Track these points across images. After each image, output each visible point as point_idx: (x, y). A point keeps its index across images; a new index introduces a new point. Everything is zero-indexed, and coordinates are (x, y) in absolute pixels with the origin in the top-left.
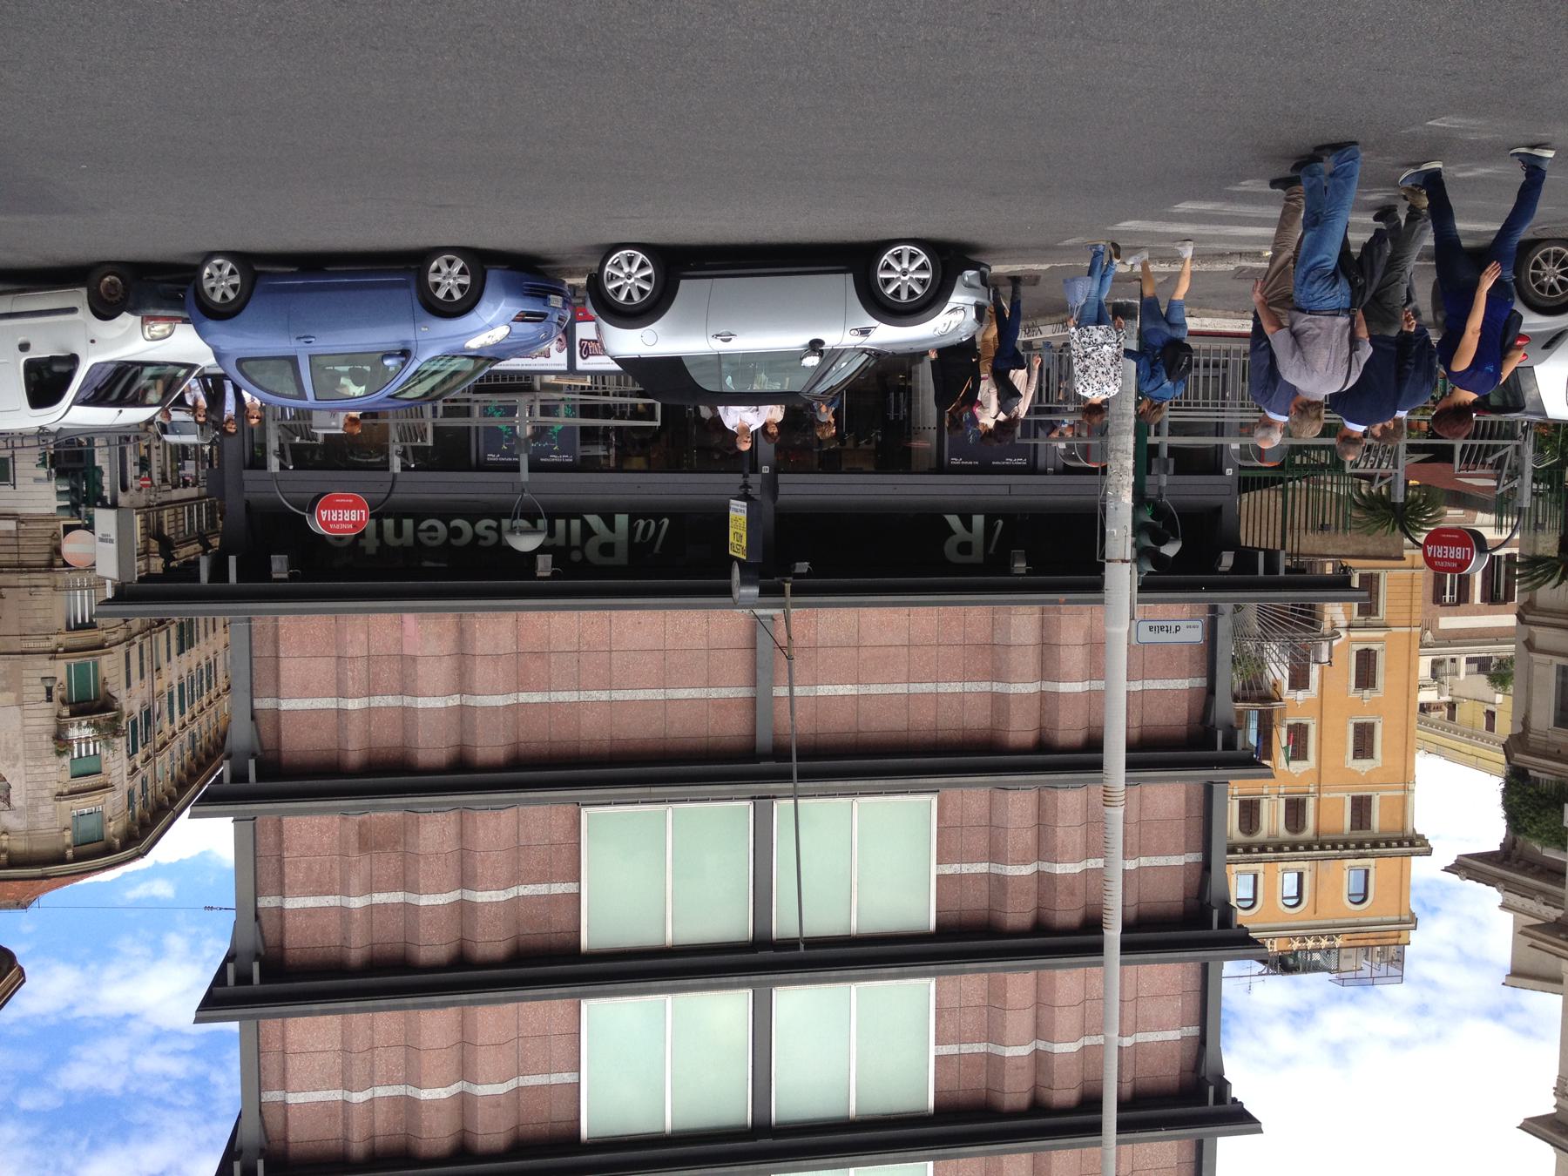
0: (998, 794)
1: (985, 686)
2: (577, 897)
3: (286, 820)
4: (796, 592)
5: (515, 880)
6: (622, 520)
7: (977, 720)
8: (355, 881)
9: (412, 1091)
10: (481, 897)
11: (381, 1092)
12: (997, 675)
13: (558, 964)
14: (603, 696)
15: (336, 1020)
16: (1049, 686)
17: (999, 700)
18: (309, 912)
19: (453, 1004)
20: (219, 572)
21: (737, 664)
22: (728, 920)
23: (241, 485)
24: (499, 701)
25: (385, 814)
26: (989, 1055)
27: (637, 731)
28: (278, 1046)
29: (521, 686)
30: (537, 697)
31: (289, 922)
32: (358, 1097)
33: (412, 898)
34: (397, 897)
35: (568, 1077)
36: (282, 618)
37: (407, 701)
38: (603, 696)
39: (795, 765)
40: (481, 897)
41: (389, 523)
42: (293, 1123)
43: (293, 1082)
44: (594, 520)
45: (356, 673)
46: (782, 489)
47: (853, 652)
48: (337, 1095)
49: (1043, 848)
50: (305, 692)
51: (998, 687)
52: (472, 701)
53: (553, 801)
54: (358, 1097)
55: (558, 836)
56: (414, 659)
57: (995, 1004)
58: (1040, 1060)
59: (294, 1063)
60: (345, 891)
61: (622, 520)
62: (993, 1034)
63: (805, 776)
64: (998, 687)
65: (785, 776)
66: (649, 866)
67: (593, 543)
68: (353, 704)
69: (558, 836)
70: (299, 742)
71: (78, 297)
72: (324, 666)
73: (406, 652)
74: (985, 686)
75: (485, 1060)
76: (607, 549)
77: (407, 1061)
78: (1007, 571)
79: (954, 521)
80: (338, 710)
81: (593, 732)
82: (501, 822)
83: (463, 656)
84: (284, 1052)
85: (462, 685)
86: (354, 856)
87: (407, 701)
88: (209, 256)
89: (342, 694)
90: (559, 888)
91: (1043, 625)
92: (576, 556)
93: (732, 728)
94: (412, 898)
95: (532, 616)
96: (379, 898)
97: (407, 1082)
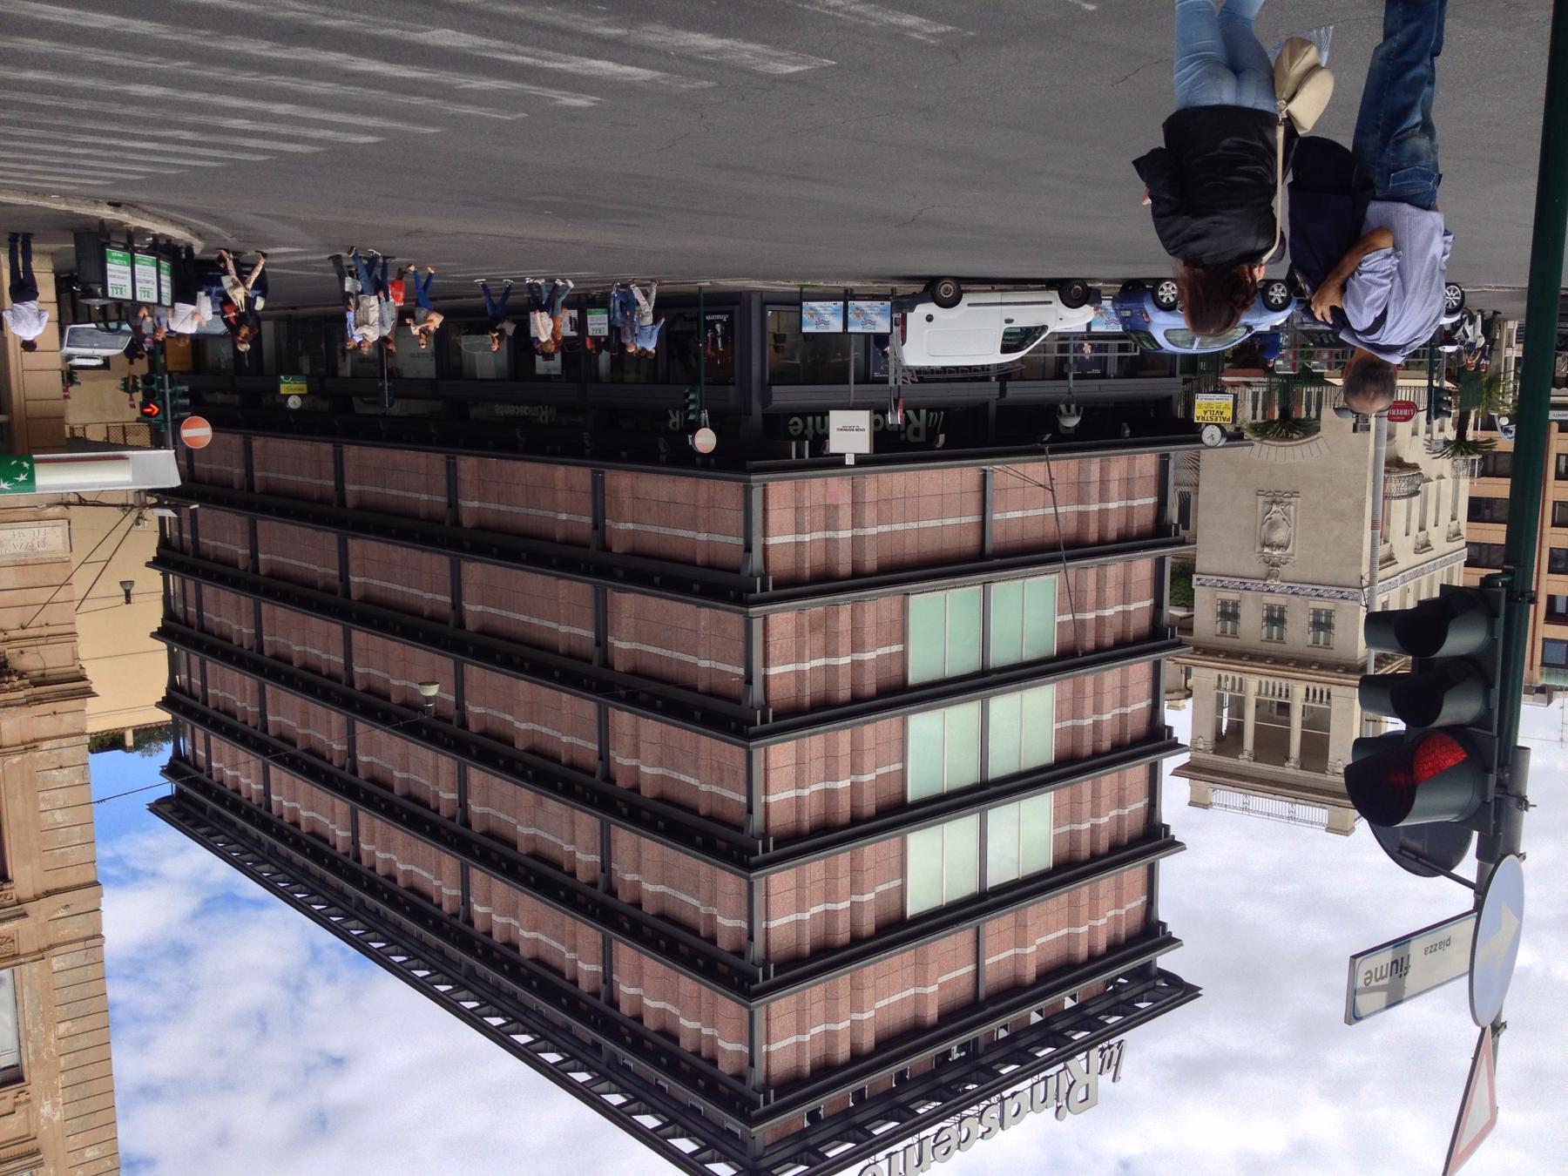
0: (1081, 572)
1: (1075, 508)
2: (904, 655)
3: (771, 617)
4: (1052, 451)
5: (879, 646)
6: (923, 412)
7: (1070, 528)
8: (807, 652)
9: (830, 785)
10: (868, 656)
11: (814, 788)
12: (1081, 500)
13: (901, 695)
14: (914, 525)
15: (792, 744)
16: (1104, 506)
17: (1082, 517)
18: (781, 676)
19: (846, 727)
20: (800, 454)
21: (973, 501)
22: (964, 661)
23: (766, 398)
24: (872, 531)
25: (815, 608)
26: (1073, 727)
27: (930, 546)
29: (880, 522)
30: (885, 528)
31: (772, 683)
32: (806, 792)
33: (832, 661)
34: (821, 662)
35: (898, 766)
36: (829, 480)
37: (830, 534)
38: (914, 525)
39: (1063, 553)
40: (868, 656)
41: (818, 419)
42: (772, 814)
43: (772, 787)
44: (911, 413)
46: (1009, 392)
47: (1020, 491)
49: (1100, 604)
50: (781, 533)
51: (1081, 508)
52: (860, 532)
53: (888, 594)
54: (806, 792)
55: (894, 617)
56: (836, 507)
57: (1078, 693)
58: (1097, 725)
59: (773, 776)
60: (800, 658)
61: (923, 412)
62: (1076, 713)
63: (1070, 558)
64: (1081, 508)
65: (1058, 560)
66: (940, 628)
67: (911, 428)
68: (807, 538)
69: (894, 617)
70: (781, 563)
71: (1054, 295)
72: (789, 514)
73: (829, 502)
74: (1075, 508)
75: (868, 759)
76: (916, 432)
77: (826, 766)
78: (1119, 434)
79: (1063, 407)
80: (797, 543)
81: (910, 549)
82: (878, 606)
83: (856, 504)
84: (766, 770)
85: (856, 523)
86: (807, 635)
87: (830, 534)
88: (1161, 280)
89: (799, 531)
90: (897, 648)
91: (1102, 469)
92: (903, 437)
93: (970, 541)
94: (832, 661)
95: (884, 476)
96: (815, 663)
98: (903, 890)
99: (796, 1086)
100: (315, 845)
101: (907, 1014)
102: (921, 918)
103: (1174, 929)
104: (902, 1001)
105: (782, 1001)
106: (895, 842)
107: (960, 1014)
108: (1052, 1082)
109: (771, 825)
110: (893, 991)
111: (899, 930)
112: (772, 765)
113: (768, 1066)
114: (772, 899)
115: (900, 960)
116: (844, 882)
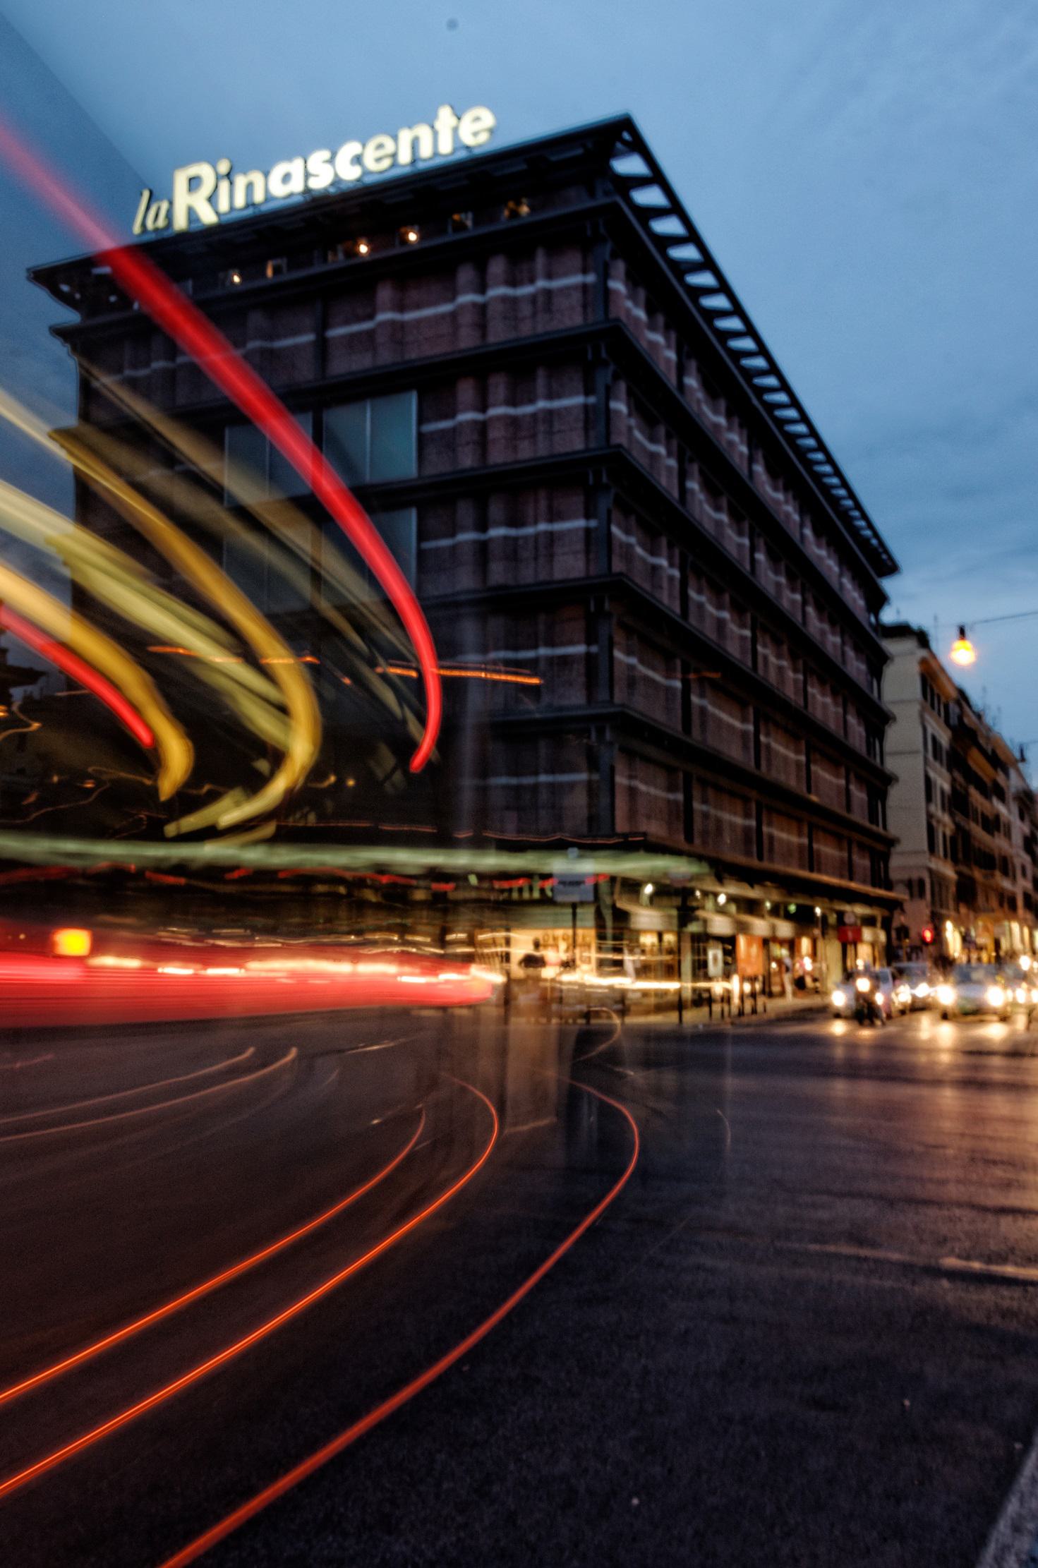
9: (512, 532)
11: (530, 530)
15: (558, 575)
28: (592, 556)
32: (543, 527)
35: (427, 545)
37: (514, 781)
43: (581, 534)
45: (544, 796)
48: (558, 526)
56: (507, 808)
59: (580, 546)
68: (543, 778)
87: (514, 781)
89: (552, 787)
97: (516, 539)
98: (421, 420)
99: (559, 238)
100: (825, 531)
101: (414, 295)
102: (405, 389)
103: (60, 349)
104: (418, 306)
105: (568, 323)
106: (430, 470)
107: (357, 285)
108: (240, 202)
109: (582, 498)
110: (431, 319)
111: (433, 381)
112: (581, 556)
113: (584, 259)
114: (581, 425)
115: (421, 351)
116: (495, 433)
